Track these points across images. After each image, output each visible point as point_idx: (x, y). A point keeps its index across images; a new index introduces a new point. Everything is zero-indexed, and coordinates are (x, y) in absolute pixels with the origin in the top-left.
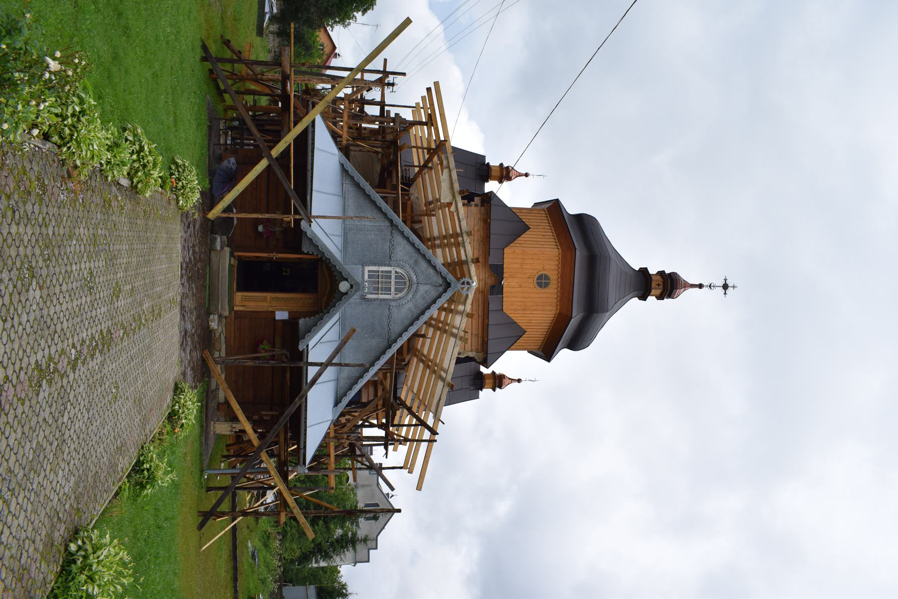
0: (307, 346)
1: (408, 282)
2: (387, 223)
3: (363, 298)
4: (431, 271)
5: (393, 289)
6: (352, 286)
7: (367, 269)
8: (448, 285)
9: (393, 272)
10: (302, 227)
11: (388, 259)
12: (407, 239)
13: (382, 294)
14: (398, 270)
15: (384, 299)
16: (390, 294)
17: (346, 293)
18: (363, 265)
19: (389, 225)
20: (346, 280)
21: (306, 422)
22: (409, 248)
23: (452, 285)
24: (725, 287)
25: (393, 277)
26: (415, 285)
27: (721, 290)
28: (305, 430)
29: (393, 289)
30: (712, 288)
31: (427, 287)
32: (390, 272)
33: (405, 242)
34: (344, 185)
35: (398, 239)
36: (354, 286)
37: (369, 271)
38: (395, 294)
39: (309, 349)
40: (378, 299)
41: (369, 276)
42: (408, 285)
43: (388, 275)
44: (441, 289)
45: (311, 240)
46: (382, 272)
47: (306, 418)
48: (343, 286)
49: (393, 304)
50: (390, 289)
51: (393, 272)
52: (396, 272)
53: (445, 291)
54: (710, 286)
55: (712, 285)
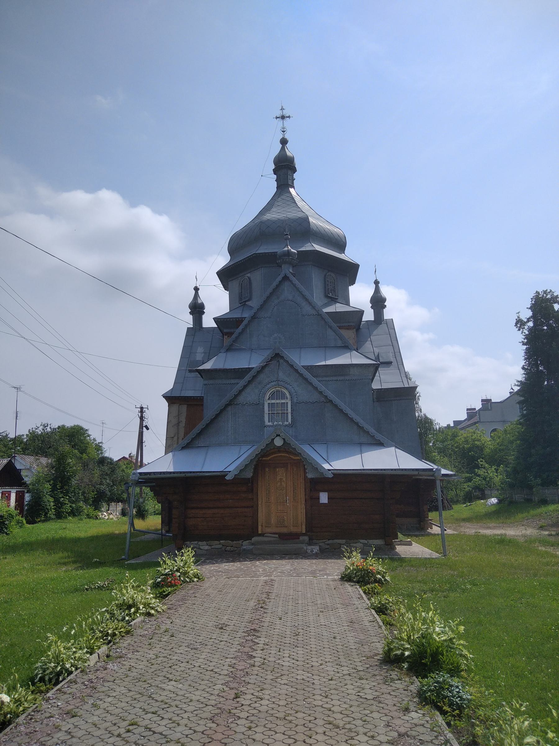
0: (329, 470)
1: (277, 389)
2: (229, 408)
5: (283, 401)
6: (278, 435)
7: (267, 423)
9: (269, 402)
10: (231, 479)
11: (259, 406)
12: (240, 392)
13: (287, 410)
14: (267, 398)
15: (292, 408)
16: (287, 403)
17: (284, 439)
19: (230, 407)
20: (273, 440)
21: (395, 470)
22: (248, 390)
23: (277, 352)
24: (283, 117)
25: (273, 401)
26: (279, 383)
27: (287, 121)
28: (402, 470)
29: (283, 401)
30: (285, 130)
31: (281, 374)
33: (243, 393)
34: (199, 445)
35: (241, 399)
36: (277, 433)
38: (287, 399)
39: (333, 468)
40: (292, 413)
42: (279, 389)
43: (271, 406)
44: (281, 361)
45: (241, 471)
46: (269, 411)
47: (392, 470)
48: (278, 442)
51: (269, 402)
54: (283, 132)
55: (282, 130)
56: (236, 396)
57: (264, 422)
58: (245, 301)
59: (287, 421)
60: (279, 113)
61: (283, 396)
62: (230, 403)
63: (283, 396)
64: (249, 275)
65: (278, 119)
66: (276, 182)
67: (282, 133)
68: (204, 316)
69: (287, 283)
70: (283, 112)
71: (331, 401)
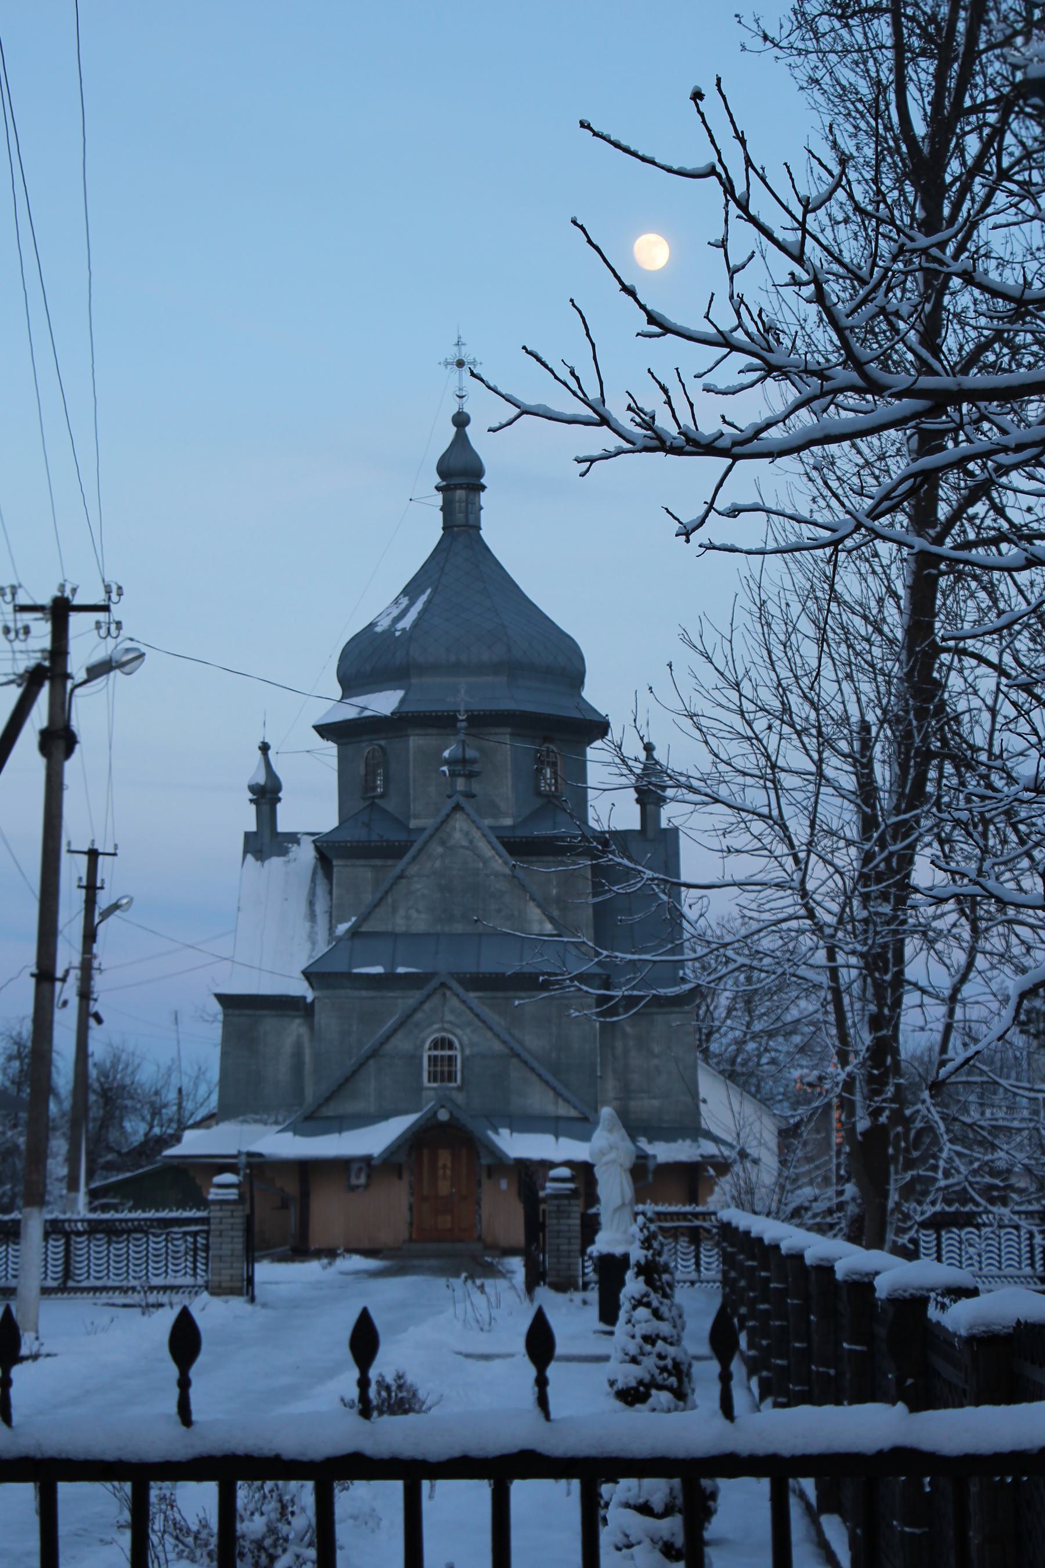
2: (371, 1062)
3: (459, 1089)
4: (426, 1007)
5: (450, 1053)
6: (443, 1107)
8: (443, 985)
11: (414, 1059)
14: (427, 1045)
18: (421, 1089)
20: (435, 1113)
22: (399, 1035)
29: (450, 1053)
32: (429, 1057)
33: (392, 1039)
35: (388, 1047)
37: (429, 1081)
41: (435, 1081)
43: (433, 1059)
44: (448, 993)
48: (443, 1115)
49: (467, 1052)
50: (450, 1058)
52: (430, 1049)
53: (450, 988)
56: (382, 1044)
57: (422, 1082)
58: (374, 797)
59: (456, 1081)
60: (452, 353)
61: (451, 1046)
62: (374, 1054)
63: (451, 1046)
64: (382, 743)
65: (449, 367)
66: (441, 514)
67: (458, 399)
68: (279, 806)
69: (458, 816)
70: (460, 352)
71: (518, 1056)
